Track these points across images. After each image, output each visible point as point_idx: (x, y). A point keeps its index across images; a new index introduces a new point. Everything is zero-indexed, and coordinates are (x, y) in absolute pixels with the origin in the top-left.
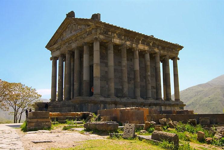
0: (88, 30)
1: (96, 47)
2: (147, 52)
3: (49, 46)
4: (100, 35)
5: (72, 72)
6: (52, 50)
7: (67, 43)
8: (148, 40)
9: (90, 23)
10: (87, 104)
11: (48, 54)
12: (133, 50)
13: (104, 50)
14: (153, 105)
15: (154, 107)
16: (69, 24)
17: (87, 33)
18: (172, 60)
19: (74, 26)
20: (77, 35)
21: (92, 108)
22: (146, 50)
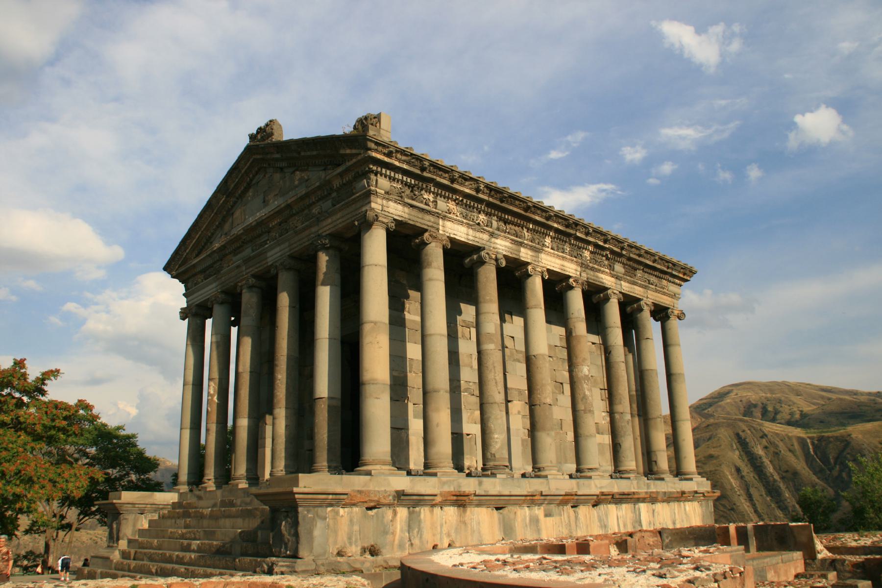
0: (336, 183)
1: (376, 249)
2: (574, 284)
3: (177, 266)
4: (391, 204)
6: (190, 278)
8: (578, 234)
9: (348, 151)
10: (329, 509)
14: (610, 503)
15: (612, 507)
17: (334, 195)
18: (657, 321)
19: (277, 176)
20: (289, 206)
21: (356, 528)
22: (570, 277)
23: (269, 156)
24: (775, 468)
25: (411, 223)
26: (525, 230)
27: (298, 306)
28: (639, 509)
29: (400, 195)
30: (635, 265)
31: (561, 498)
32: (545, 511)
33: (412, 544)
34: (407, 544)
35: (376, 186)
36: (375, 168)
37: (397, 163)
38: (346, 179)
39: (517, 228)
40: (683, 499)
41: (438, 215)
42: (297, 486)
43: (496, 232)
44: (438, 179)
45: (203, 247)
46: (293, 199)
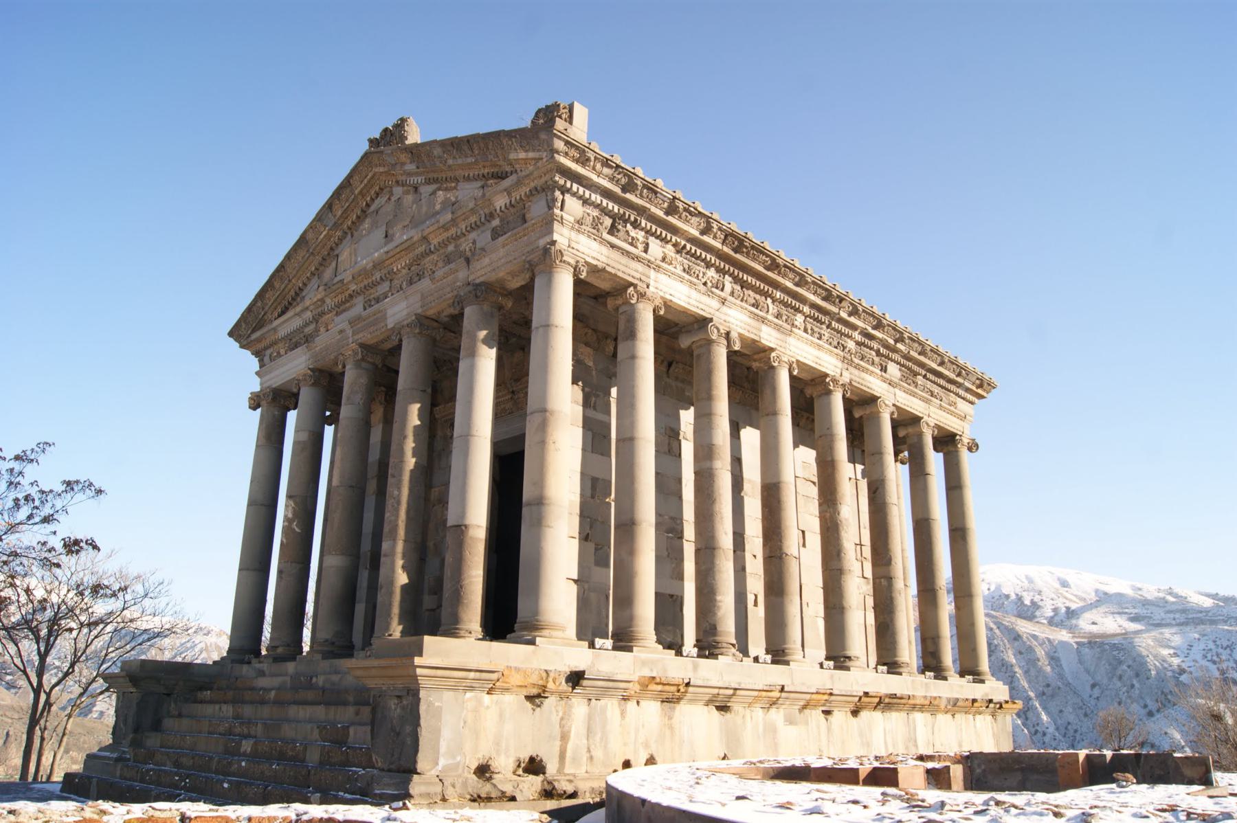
0: (500, 202)
3: (249, 330)
4: (583, 239)
5: (372, 486)
6: (266, 349)
7: (359, 301)
9: (522, 155)
10: (469, 695)
11: (243, 372)
12: (755, 365)
13: (587, 344)
15: (877, 715)
16: (381, 189)
17: (496, 222)
19: (409, 198)
20: (425, 239)
22: (826, 375)
23: (398, 167)
24: (1029, 682)
25: (608, 269)
26: (769, 301)
27: (429, 390)
28: (914, 721)
29: (596, 224)
30: (916, 368)
31: (808, 697)
32: (785, 716)
33: (591, 758)
34: (585, 756)
35: (562, 210)
36: (562, 182)
37: (594, 177)
38: (516, 195)
39: (758, 297)
40: (974, 709)
41: (649, 264)
42: (421, 655)
43: (730, 298)
44: (653, 209)
45: (290, 304)
46: (432, 229)
